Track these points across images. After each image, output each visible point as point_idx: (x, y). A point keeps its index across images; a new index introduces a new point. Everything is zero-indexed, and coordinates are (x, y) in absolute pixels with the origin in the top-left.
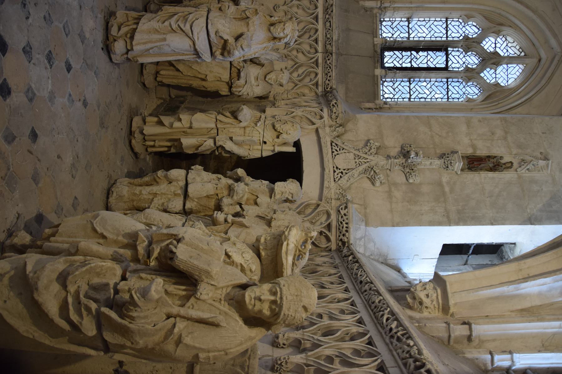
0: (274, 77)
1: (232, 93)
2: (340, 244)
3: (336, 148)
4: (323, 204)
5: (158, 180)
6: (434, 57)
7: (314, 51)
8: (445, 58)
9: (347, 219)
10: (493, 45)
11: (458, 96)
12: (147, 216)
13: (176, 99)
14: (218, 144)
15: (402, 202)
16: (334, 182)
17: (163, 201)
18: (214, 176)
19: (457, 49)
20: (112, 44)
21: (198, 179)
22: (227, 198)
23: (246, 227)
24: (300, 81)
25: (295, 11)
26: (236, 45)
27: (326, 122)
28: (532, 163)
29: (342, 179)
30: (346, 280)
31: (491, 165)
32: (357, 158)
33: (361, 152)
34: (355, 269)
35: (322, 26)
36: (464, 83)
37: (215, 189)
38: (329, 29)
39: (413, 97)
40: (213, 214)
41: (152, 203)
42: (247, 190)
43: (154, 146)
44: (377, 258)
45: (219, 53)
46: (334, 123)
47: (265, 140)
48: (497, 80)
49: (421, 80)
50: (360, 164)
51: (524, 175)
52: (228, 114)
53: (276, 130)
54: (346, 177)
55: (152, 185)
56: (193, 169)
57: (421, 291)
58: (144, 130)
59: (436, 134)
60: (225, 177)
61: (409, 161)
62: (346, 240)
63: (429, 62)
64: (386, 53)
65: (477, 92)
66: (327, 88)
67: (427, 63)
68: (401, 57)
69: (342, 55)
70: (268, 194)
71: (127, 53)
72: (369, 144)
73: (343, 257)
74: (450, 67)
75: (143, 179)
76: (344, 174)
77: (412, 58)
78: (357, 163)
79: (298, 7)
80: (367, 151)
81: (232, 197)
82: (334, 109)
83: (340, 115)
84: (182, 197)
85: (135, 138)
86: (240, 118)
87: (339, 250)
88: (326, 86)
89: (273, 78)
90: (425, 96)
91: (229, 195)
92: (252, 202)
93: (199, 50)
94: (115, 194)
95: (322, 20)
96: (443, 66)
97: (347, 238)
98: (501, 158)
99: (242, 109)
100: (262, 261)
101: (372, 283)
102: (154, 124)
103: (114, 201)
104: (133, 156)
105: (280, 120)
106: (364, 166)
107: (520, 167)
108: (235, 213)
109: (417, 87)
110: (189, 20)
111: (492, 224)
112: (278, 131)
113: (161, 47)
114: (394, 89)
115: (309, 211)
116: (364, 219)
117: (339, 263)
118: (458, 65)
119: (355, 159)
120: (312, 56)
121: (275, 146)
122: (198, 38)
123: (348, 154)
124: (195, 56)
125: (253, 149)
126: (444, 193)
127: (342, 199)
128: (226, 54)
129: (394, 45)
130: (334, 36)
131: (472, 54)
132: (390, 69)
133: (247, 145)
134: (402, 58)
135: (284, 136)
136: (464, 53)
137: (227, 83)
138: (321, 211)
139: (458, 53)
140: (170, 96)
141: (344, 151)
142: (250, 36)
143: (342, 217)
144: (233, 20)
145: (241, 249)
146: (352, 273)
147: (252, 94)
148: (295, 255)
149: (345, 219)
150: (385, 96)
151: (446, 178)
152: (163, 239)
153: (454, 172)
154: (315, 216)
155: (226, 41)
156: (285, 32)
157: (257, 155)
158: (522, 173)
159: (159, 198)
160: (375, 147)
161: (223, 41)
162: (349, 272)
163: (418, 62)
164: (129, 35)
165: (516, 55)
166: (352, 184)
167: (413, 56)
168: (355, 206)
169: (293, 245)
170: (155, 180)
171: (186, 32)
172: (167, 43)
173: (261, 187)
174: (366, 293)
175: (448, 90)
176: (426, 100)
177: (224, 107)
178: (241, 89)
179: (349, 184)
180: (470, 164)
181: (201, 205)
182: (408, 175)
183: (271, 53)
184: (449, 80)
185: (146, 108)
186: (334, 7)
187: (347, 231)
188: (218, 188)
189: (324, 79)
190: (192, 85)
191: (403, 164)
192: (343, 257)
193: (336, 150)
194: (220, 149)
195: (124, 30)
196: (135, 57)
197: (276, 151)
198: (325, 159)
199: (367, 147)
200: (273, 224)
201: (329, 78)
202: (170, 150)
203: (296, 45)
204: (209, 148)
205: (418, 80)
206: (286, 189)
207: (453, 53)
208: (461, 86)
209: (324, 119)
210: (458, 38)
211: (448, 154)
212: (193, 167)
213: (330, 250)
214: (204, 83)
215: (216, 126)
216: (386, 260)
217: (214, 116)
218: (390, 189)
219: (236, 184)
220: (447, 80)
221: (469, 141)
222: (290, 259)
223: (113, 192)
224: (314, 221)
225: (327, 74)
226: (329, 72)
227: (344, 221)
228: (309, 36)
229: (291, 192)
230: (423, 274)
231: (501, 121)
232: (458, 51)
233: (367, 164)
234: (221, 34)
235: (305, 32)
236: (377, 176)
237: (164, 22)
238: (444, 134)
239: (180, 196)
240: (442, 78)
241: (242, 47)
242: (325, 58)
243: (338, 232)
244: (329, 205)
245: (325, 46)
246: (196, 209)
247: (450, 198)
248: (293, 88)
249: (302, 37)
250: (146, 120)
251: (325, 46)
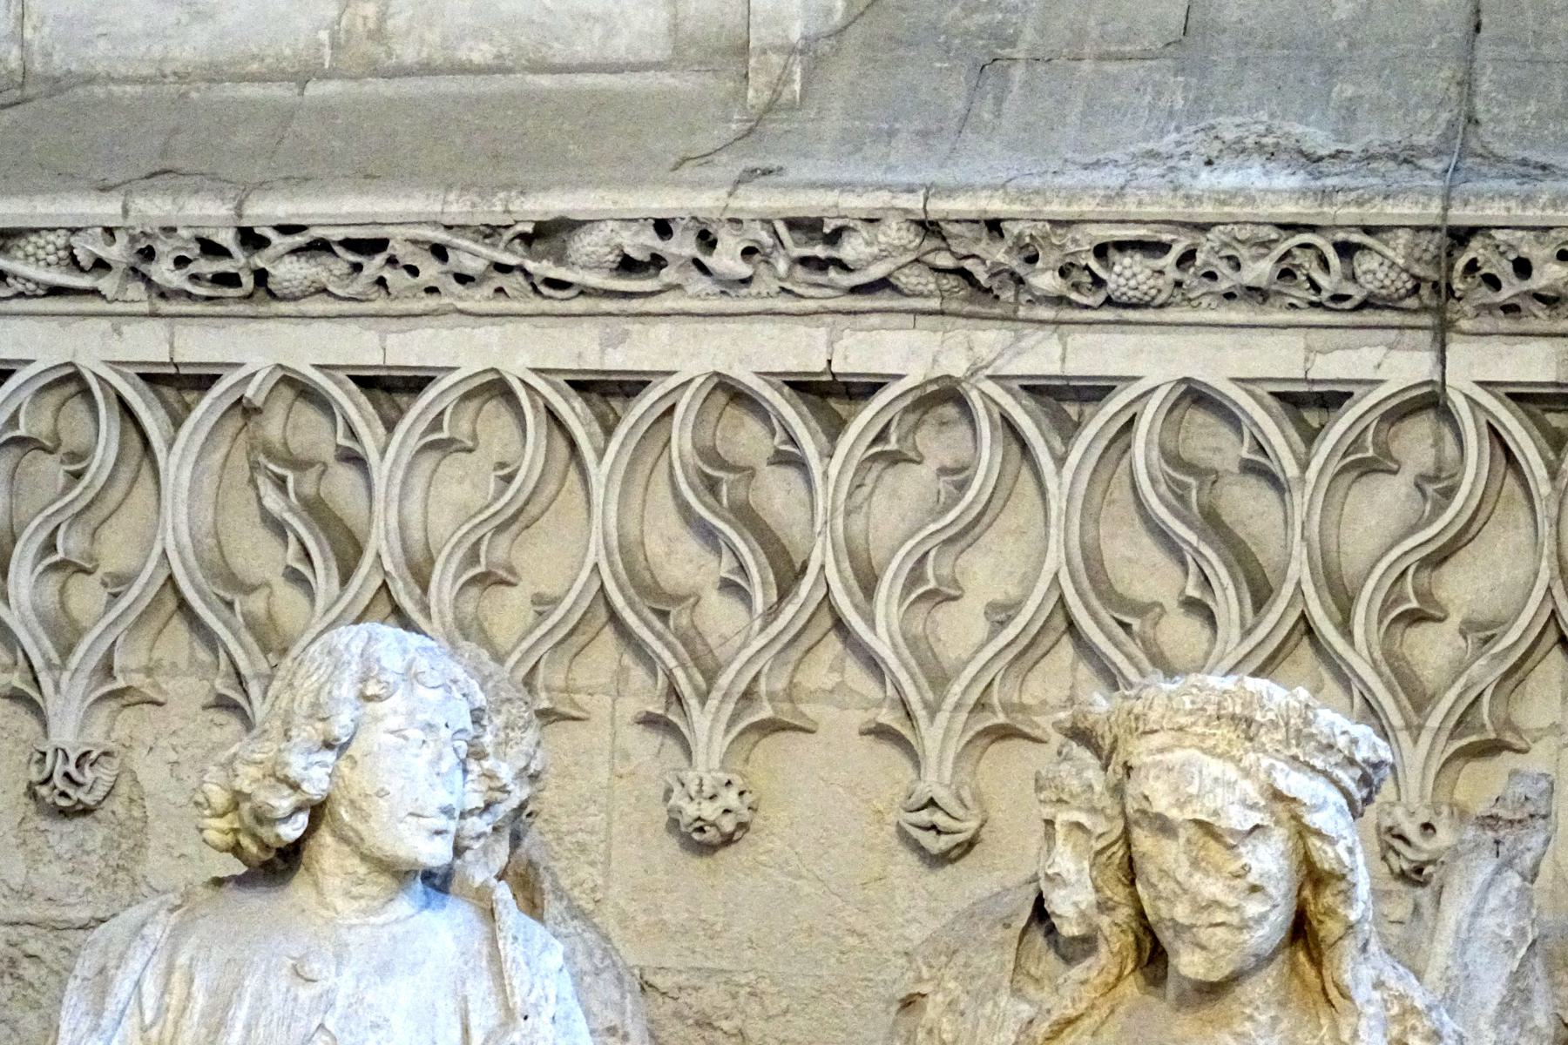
25: (981, 628)
35: (1156, 339)
38: (1188, 257)
69: (1472, 120)
79: (937, 597)
95: (1080, 339)
120: (1476, 451)
130: (1264, 210)
156: (1237, 819)
183: (1441, 952)
186: (940, 207)
203: (1346, 630)
228: (1252, 480)
235: (1213, 523)
242: (1510, 309)
249: (1267, 556)
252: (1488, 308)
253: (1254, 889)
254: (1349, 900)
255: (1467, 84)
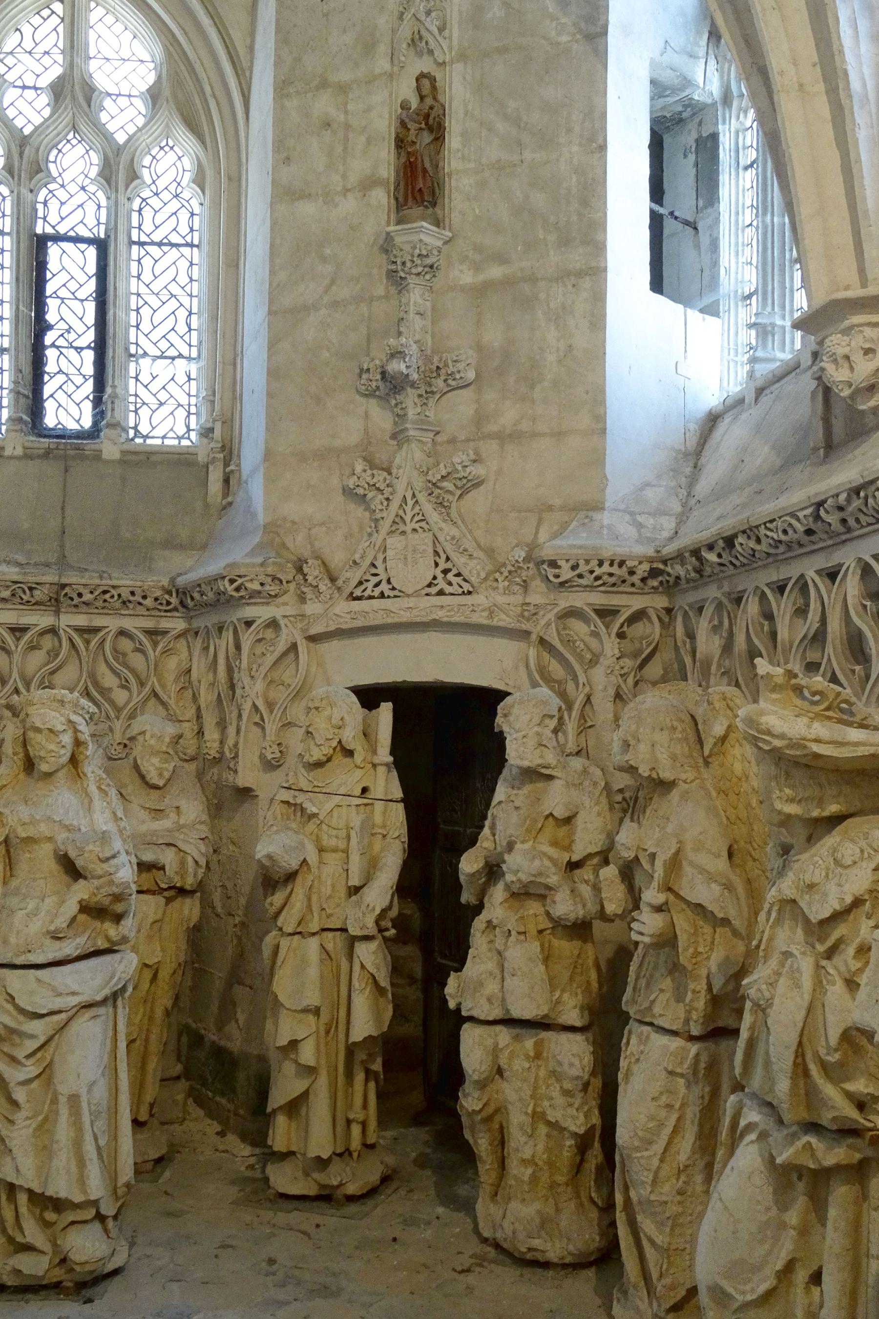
0: (155, 761)
1: (201, 886)
2: (655, 583)
3: (370, 585)
4: (539, 627)
5: (490, 1110)
6: (63, 277)
7: (49, 637)
8: (67, 246)
9: (587, 562)
10: (30, 94)
11: (184, 215)
12: (641, 1139)
13: (183, 1058)
14: (371, 929)
15: (533, 402)
16: (474, 596)
17: (556, 1093)
18: (478, 940)
19: (40, 207)
20: (78, 1269)
21: (492, 987)
22: (554, 902)
23: (678, 852)
24: (142, 684)
26: (100, 877)
27: (290, 611)
28: (423, 18)
29: (466, 573)
30: (792, 571)
31: (427, 138)
32: (402, 527)
33: (384, 514)
34: (758, 547)
36: (144, 195)
37: (522, 937)
39: (185, 351)
40: (645, 944)
41: (564, 1125)
42: (528, 846)
43: (364, 1124)
44: (683, 481)
45: (114, 926)
46: (292, 586)
47: (358, 792)
48: (138, 94)
49: (133, 322)
50: (420, 517)
51: (455, 43)
52: (278, 898)
53: (329, 760)
54: (459, 560)
55: (501, 1128)
56: (459, 1004)
57: (852, 369)
58: (319, 1158)
59: (326, 292)
60: (479, 908)
61: (415, 376)
62: (646, 567)
63: (81, 295)
64: (50, 421)
65: (171, 157)
66: (168, 603)
67: (82, 301)
68: (61, 378)
70: (540, 785)
71: (100, 1218)
72: (360, 491)
73: (702, 576)
74: (95, 231)
75: (484, 1155)
76: (449, 565)
77: (66, 344)
78: (417, 526)
80: (380, 497)
81: (550, 888)
82: (248, 585)
83: (270, 570)
84: (544, 1034)
85: (341, 1185)
86: (294, 864)
87: (672, 587)
88: (163, 607)
89: (157, 765)
90: (182, 314)
91: (543, 897)
92: (562, 832)
93: (107, 992)
94: (536, 1243)
96: (92, 252)
97: (640, 563)
98: (405, 106)
99: (269, 857)
100: (852, 810)
101: (820, 504)
102: (293, 1124)
103: (558, 1245)
104: (389, 1191)
105: (279, 744)
106: (428, 507)
107: (431, 52)
108: (623, 881)
109: (154, 336)
110: (12, 1024)
111: (603, 148)
112: (331, 751)
113: (93, 1108)
114: (161, 404)
115: (556, 669)
116: (582, 514)
117: (720, 587)
118: (91, 207)
119: (403, 533)
121: (376, 761)
122: (74, 994)
123: (390, 553)
124: (119, 1002)
125: (384, 827)
126: (508, 282)
127: (524, 574)
128: (119, 908)
129: (27, 397)
130: (8, 577)
131: (55, 162)
132: (99, 414)
133: (370, 845)
134: (67, 375)
135: (350, 736)
136: (51, 187)
137: (169, 900)
138: (559, 634)
139: (53, 204)
140: (178, 1078)
141: (379, 563)
142: (64, 835)
143: (580, 576)
144: (14, 883)
145: (828, 869)
146: (768, 554)
147: (203, 827)
148: (840, 721)
149: (588, 567)
150: (180, 434)
151: (461, 271)
152: (802, 1092)
153: (445, 249)
154: (574, 650)
155: (85, 908)
156: (60, 728)
157: (398, 813)
158: (451, 48)
159: (546, 1103)
160: (369, 472)
161: (82, 917)
162: (760, 563)
163: (79, 327)
164: (51, 1216)
165: (60, 29)
166: (479, 545)
167: (61, 342)
168: (543, 536)
169: (816, 725)
170: (489, 1119)
171: (51, 1032)
172: (83, 1093)
173: (517, 804)
174: (851, 522)
175: (165, 244)
176: (195, 310)
177: (219, 910)
178: (190, 859)
179: (481, 555)
180: (423, 201)
181: (571, 979)
182: (453, 383)
184: (135, 238)
185: (226, 1151)
187: (621, 564)
188: (522, 929)
189: (141, 610)
190: (167, 1009)
191: (420, 396)
192: (702, 576)
193: (377, 585)
194: (383, 924)
195: (32, 1233)
196: (115, 1189)
197: (391, 759)
198: (405, 620)
199: (370, 495)
200: (666, 775)
201: (138, 598)
202: (376, 1073)
204: (381, 955)
205: (133, 331)
206: (531, 734)
207: (53, 218)
208: (155, 202)
209: (278, 617)
210: (4, 198)
211: (394, 263)
212: (452, 1005)
213: (669, 611)
214: (165, 974)
215: (314, 934)
216: (686, 455)
217: (284, 943)
218: (490, 436)
219: (509, 877)
220: (135, 243)
221: (349, 194)
222: (855, 734)
223: (530, 1249)
224: (589, 656)
225: (124, 603)
226: (119, 595)
227: (592, 572)
229: (536, 720)
230: (722, 351)
231: (288, 96)
232: (45, 203)
233: (421, 497)
234: (61, 922)
236: (457, 471)
237: (15, 1104)
238: (329, 269)
239: (542, 1040)
240: (129, 259)
241: (108, 859)
242: (76, 606)
243: (621, 589)
244: (542, 613)
245: (36, 604)
246: (582, 992)
247: (524, 264)
248: (164, 704)
250: (285, 1150)
251: (36, 604)
252: (70, 606)
253: (63, 746)
254: (87, 749)
255: (62, 546)
